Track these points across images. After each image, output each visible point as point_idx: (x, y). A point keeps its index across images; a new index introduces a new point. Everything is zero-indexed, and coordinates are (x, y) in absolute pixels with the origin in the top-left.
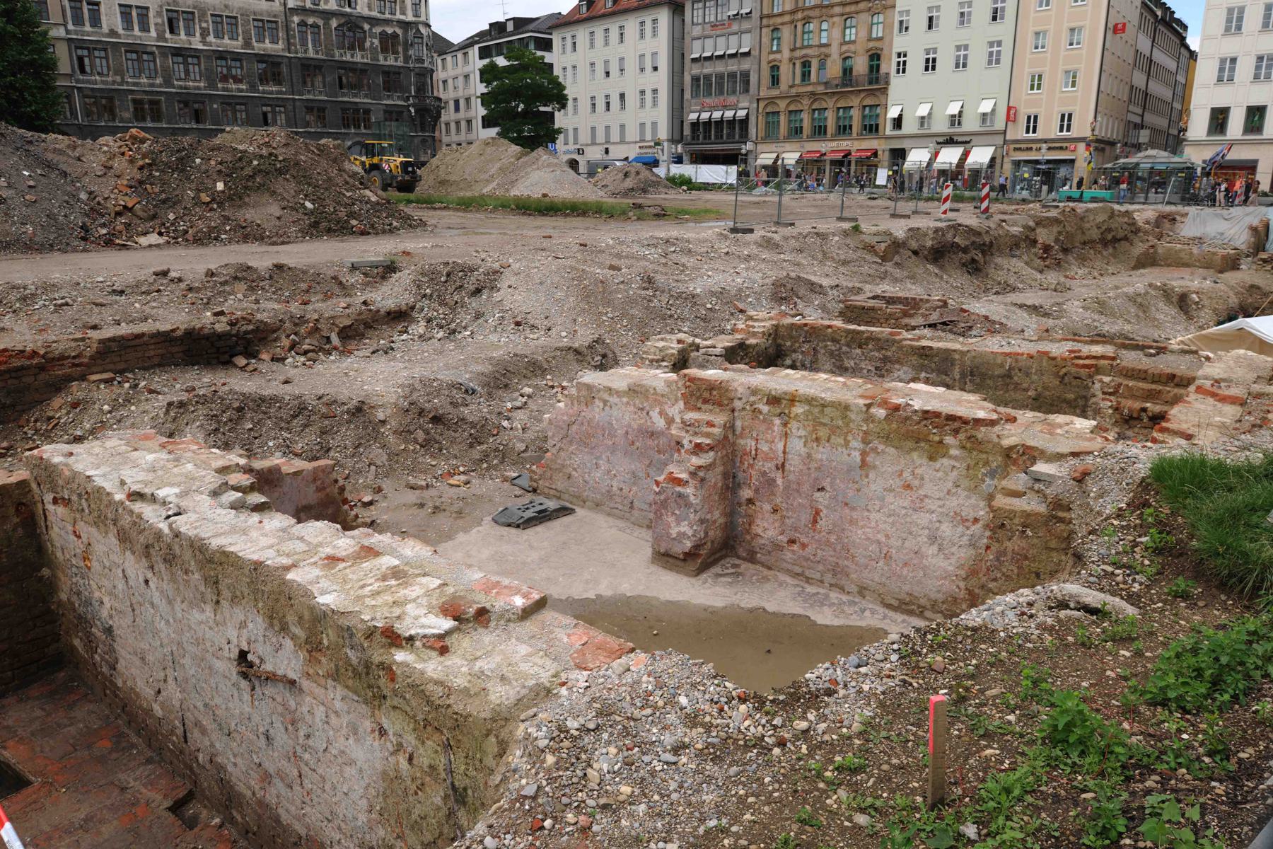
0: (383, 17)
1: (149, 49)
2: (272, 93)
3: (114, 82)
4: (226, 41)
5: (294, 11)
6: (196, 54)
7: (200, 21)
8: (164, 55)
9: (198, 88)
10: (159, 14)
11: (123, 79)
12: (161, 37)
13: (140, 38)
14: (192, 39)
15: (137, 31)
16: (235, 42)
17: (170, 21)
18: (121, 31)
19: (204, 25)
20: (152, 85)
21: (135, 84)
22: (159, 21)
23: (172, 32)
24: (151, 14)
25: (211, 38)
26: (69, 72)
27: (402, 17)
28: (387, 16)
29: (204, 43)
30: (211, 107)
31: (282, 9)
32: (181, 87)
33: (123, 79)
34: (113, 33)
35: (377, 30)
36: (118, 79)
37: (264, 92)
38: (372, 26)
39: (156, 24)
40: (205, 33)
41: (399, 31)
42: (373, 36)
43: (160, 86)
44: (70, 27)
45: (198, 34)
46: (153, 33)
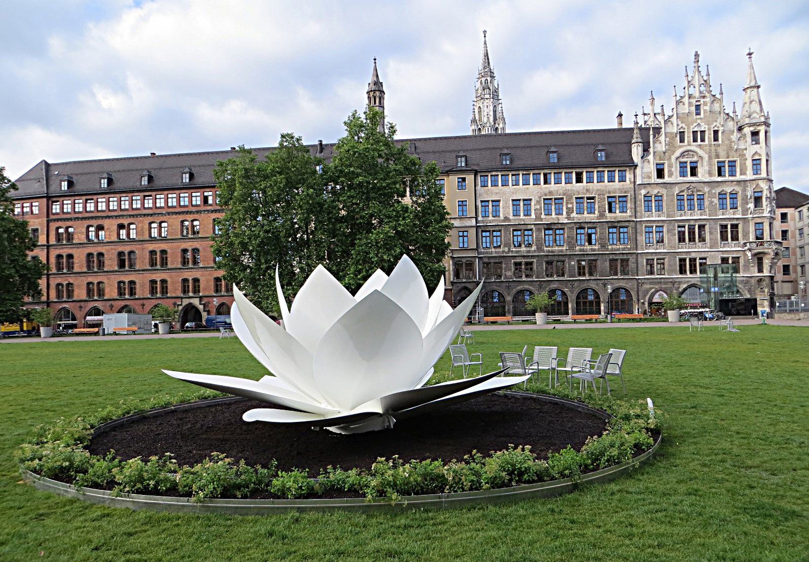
0: (720, 179)
1: (529, 227)
2: (618, 250)
3: (503, 252)
4: (586, 215)
5: (643, 185)
6: (562, 226)
7: (567, 203)
8: (539, 230)
9: (562, 251)
10: (538, 202)
11: (509, 249)
12: (538, 217)
13: (524, 220)
14: (560, 217)
15: (522, 216)
16: (592, 215)
17: (610, 204)
18: (511, 217)
19: (570, 206)
20: (529, 252)
21: (517, 252)
22: (538, 207)
23: (610, 211)
24: (533, 203)
25: (574, 215)
26: (475, 247)
27: (743, 177)
28: (727, 178)
29: (568, 218)
30: (569, 264)
31: (632, 186)
32: (549, 251)
33: (509, 249)
34: (506, 219)
36: (506, 249)
37: (612, 250)
38: (713, 188)
39: (535, 210)
40: (570, 211)
42: (712, 196)
43: (535, 251)
44: (480, 218)
45: (564, 213)
46: (533, 216)
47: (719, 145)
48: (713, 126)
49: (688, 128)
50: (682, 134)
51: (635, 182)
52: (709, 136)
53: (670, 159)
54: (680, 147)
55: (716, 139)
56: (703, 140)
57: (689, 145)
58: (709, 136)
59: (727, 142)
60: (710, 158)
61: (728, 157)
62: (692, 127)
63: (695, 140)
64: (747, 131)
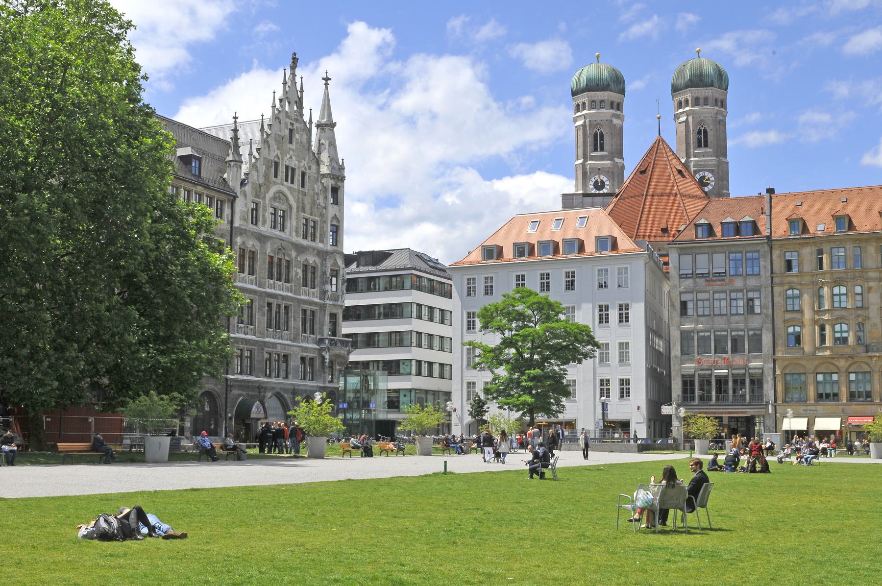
27: (321, 245)
31: (228, 227)
35: (301, 258)
41: (318, 261)
47: (304, 194)
48: (302, 165)
49: (283, 159)
50: (277, 164)
51: (232, 222)
52: (298, 177)
53: (264, 198)
54: (275, 183)
55: (303, 186)
56: (292, 182)
57: (282, 184)
58: (298, 177)
59: (312, 192)
60: (298, 208)
61: (311, 214)
62: (286, 158)
63: (286, 180)
64: (329, 183)
